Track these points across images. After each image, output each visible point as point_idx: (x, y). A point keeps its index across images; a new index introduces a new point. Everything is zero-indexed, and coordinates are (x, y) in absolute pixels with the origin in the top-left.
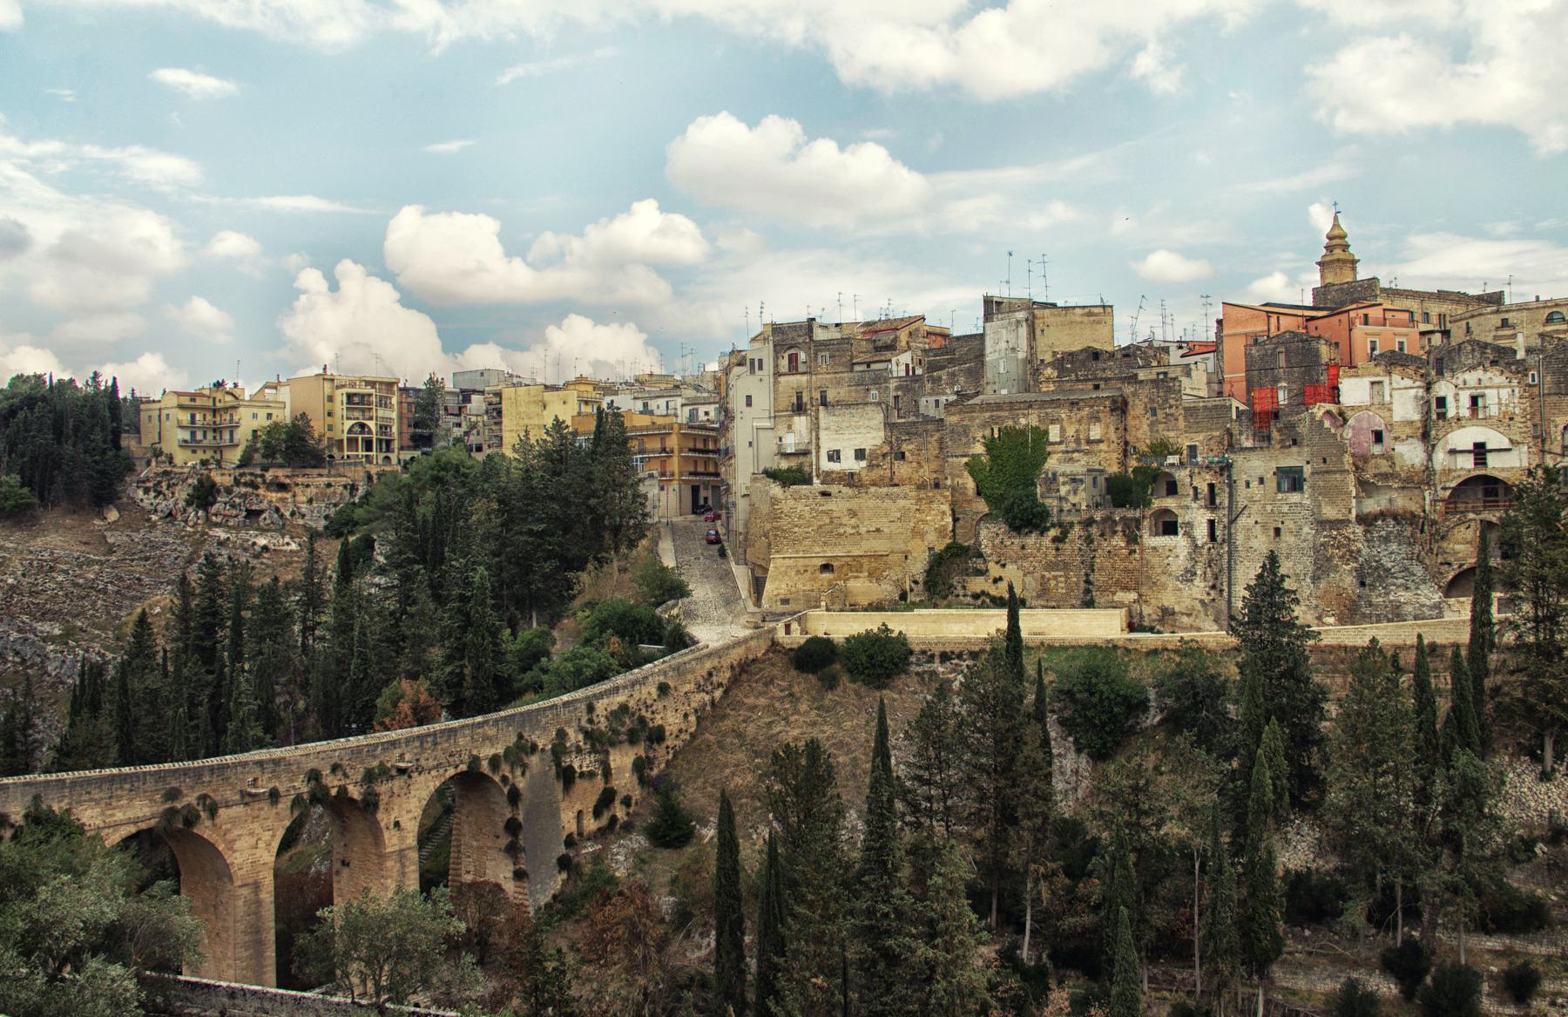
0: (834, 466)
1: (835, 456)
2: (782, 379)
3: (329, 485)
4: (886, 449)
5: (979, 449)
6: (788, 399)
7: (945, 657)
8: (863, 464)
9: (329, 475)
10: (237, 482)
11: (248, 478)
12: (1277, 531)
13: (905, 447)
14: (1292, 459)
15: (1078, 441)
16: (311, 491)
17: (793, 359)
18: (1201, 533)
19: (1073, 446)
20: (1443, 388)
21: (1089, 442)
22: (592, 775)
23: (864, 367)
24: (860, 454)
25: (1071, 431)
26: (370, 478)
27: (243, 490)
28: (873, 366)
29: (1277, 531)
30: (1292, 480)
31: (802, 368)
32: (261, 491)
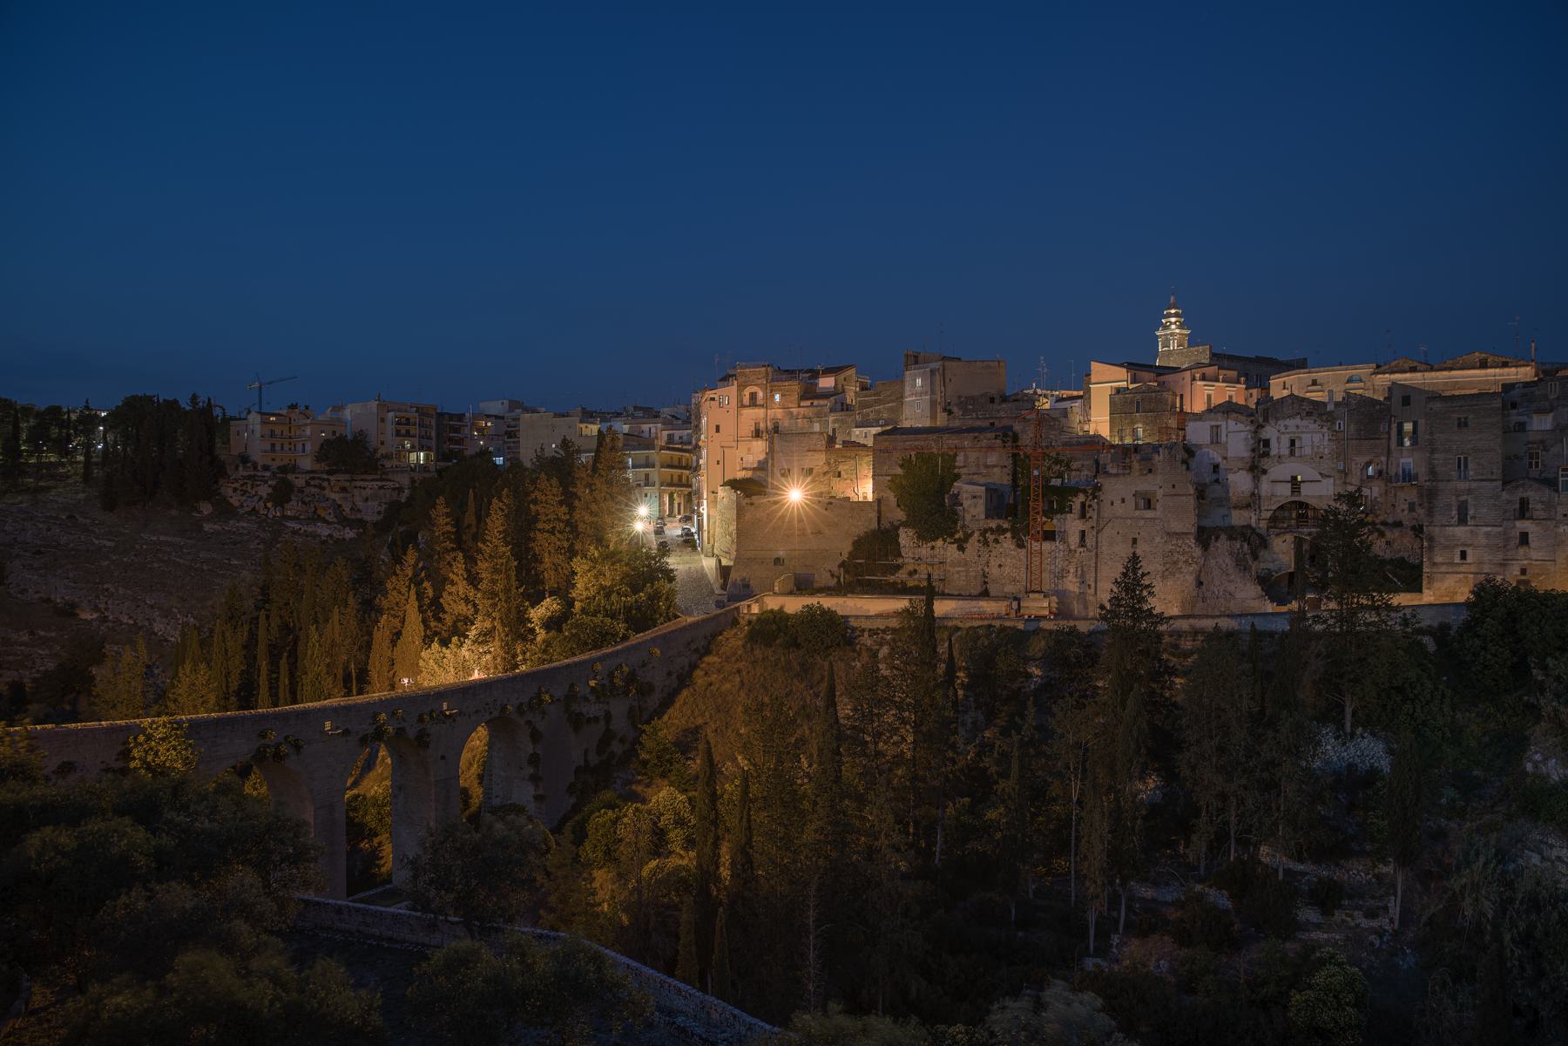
2: (746, 412)
3: (381, 488)
4: (826, 468)
6: (747, 428)
7: (873, 632)
9: (381, 480)
10: (308, 484)
11: (316, 482)
13: (841, 468)
15: (978, 465)
16: (368, 492)
18: (1074, 540)
19: (973, 470)
20: (1269, 432)
21: (987, 467)
22: (596, 719)
26: (413, 481)
27: (313, 490)
29: (1135, 541)
32: (327, 492)
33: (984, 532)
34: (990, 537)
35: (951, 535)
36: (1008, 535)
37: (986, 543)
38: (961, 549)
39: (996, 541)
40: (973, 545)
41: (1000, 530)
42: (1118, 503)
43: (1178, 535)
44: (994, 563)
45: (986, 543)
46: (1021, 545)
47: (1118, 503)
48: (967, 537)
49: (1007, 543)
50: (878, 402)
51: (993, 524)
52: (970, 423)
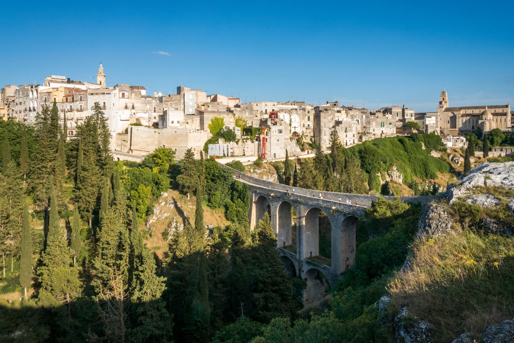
0: (172, 125)
1: (173, 122)
5: (211, 123)
8: (179, 124)
14: (281, 128)
17: (123, 95)
23: (144, 99)
24: (178, 122)
25: (227, 120)
28: (147, 99)
30: (280, 132)
31: (126, 96)
33: (243, 139)
34: (245, 141)
37: (244, 142)
38: (237, 144)
40: (240, 143)
41: (247, 139)
43: (287, 139)
44: (246, 147)
45: (244, 142)
46: (253, 142)
48: (239, 140)
49: (249, 142)
50: (171, 100)
51: (245, 137)
52: (213, 110)
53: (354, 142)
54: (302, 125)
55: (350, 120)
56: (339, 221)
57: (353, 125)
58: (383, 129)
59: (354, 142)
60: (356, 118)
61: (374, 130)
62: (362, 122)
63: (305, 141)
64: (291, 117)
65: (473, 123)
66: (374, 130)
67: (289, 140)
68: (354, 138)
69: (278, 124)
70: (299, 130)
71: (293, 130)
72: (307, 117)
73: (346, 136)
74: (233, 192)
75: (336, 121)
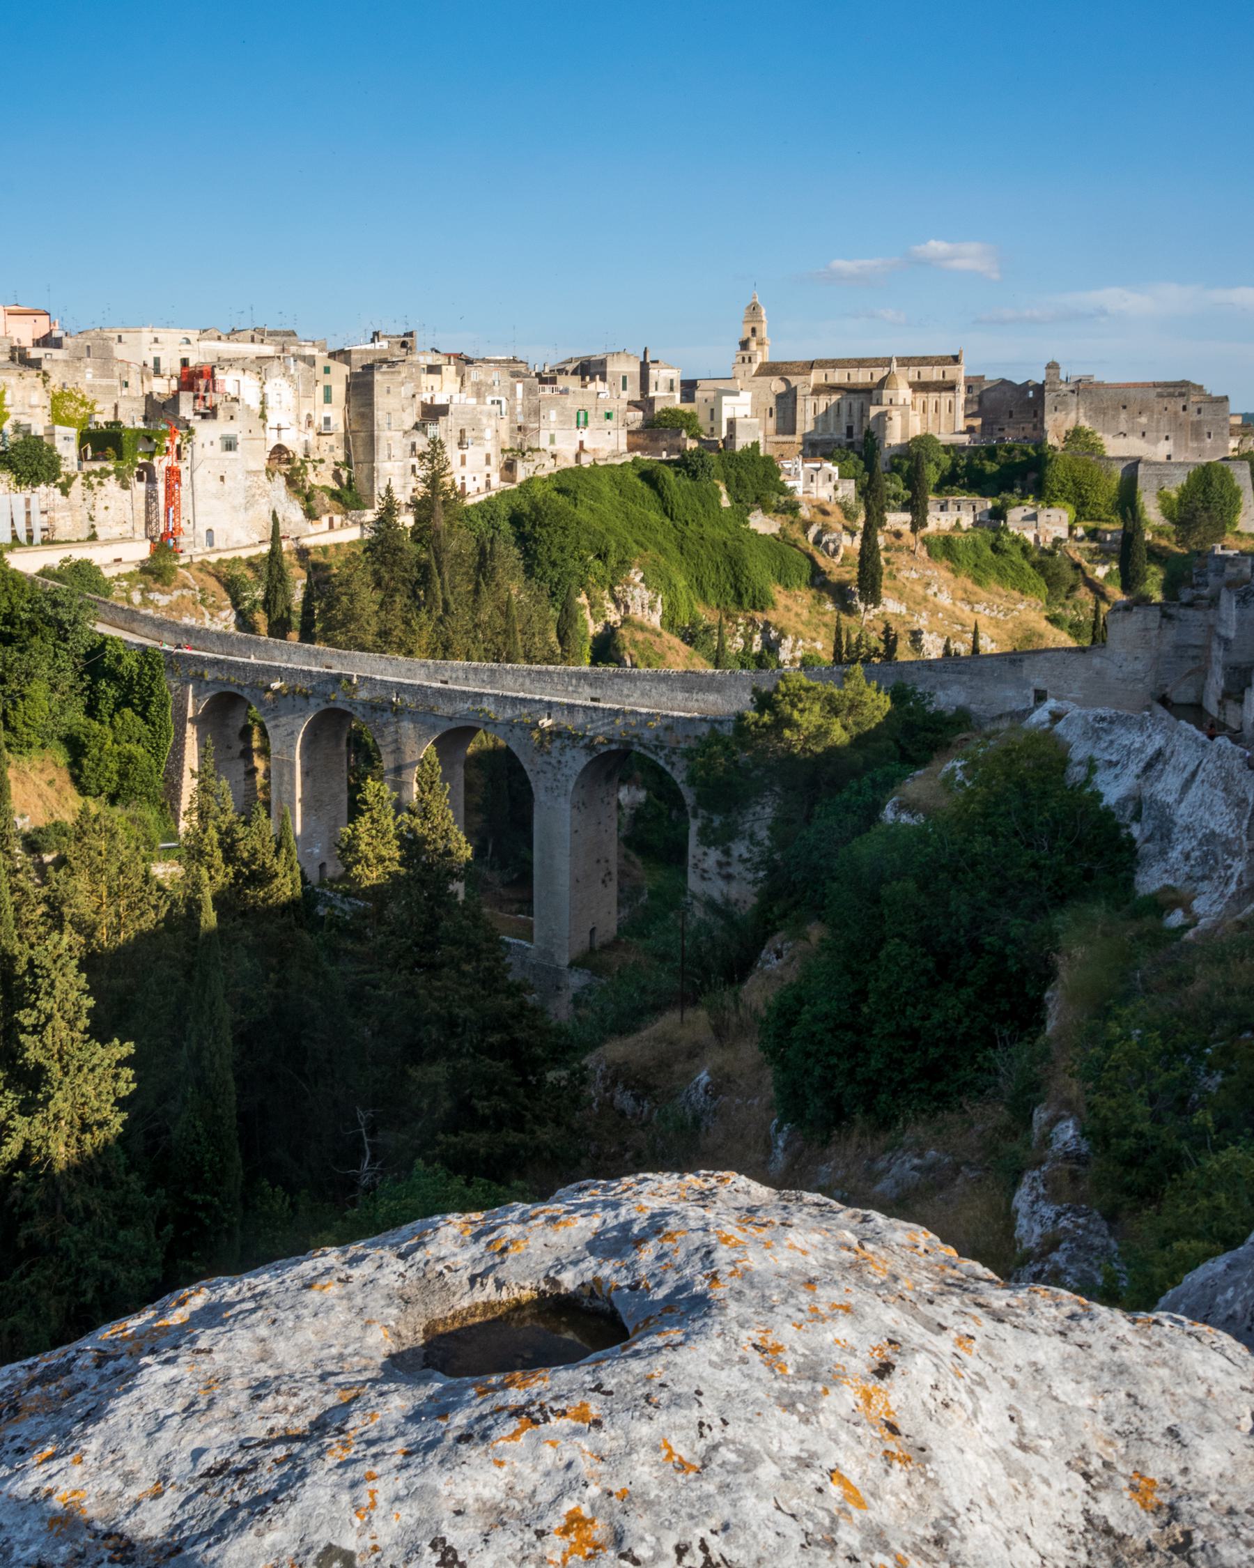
12: (222, 478)
14: (230, 429)
19: (20, 410)
21: (31, 407)
25: (18, 398)
29: (222, 478)
30: (230, 445)
34: (94, 480)
35: (54, 480)
36: (113, 477)
37: (90, 487)
38: (65, 493)
39: (100, 484)
40: (77, 488)
41: (104, 473)
42: (207, 445)
43: (255, 473)
44: (100, 505)
45: (90, 487)
46: (125, 486)
47: (207, 445)
48: (70, 480)
49: (111, 484)
51: (97, 466)
53: (488, 484)
54: (303, 419)
55: (473, 401)
56: (566, 771)
57: (484, 420)
58: (584, 435)
59: (488, 484)
60: (492, 393)
61: (552, 441)
62: (512, 409)
63: (315, 482)
64: (267, 389)
65: (850, 415)
66: (552, 441)
67: (263, 477)
68: (488, 469)
69: (221, 413)
70: (293, 441)
71: (273, 440)
72: (320, 390)
73: (463, 463)
74: (95, 681)
75: (424, 405)
